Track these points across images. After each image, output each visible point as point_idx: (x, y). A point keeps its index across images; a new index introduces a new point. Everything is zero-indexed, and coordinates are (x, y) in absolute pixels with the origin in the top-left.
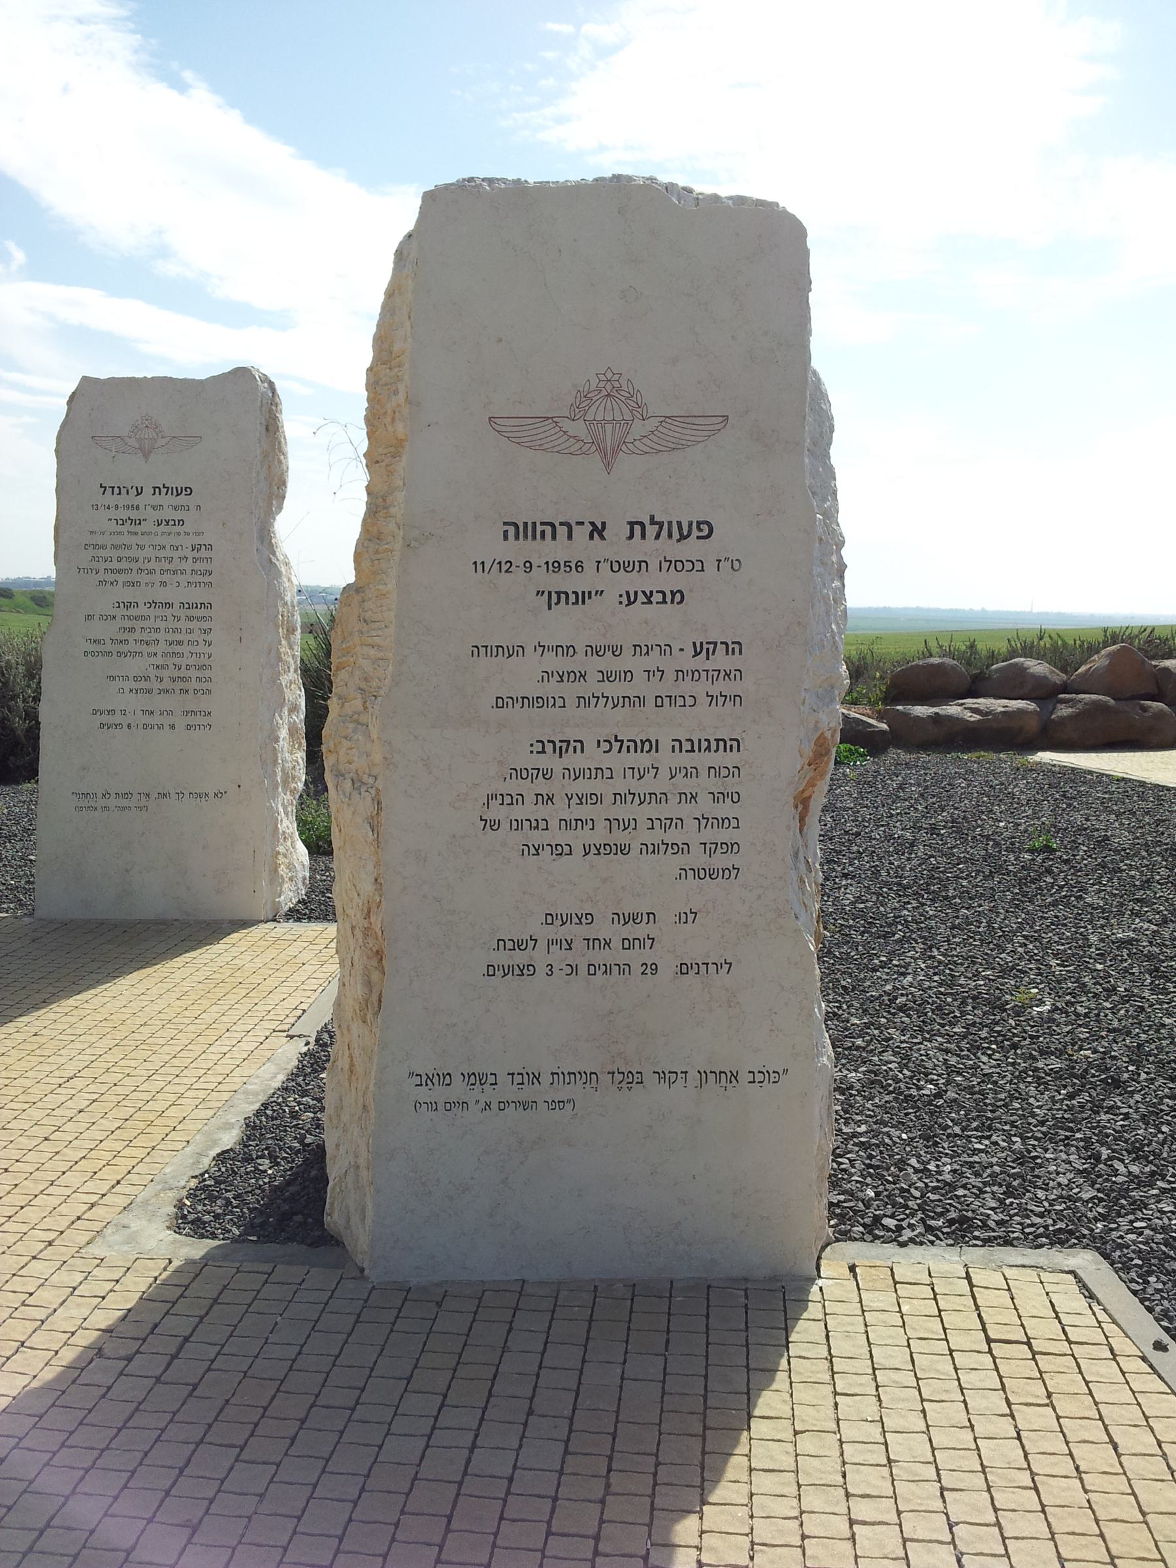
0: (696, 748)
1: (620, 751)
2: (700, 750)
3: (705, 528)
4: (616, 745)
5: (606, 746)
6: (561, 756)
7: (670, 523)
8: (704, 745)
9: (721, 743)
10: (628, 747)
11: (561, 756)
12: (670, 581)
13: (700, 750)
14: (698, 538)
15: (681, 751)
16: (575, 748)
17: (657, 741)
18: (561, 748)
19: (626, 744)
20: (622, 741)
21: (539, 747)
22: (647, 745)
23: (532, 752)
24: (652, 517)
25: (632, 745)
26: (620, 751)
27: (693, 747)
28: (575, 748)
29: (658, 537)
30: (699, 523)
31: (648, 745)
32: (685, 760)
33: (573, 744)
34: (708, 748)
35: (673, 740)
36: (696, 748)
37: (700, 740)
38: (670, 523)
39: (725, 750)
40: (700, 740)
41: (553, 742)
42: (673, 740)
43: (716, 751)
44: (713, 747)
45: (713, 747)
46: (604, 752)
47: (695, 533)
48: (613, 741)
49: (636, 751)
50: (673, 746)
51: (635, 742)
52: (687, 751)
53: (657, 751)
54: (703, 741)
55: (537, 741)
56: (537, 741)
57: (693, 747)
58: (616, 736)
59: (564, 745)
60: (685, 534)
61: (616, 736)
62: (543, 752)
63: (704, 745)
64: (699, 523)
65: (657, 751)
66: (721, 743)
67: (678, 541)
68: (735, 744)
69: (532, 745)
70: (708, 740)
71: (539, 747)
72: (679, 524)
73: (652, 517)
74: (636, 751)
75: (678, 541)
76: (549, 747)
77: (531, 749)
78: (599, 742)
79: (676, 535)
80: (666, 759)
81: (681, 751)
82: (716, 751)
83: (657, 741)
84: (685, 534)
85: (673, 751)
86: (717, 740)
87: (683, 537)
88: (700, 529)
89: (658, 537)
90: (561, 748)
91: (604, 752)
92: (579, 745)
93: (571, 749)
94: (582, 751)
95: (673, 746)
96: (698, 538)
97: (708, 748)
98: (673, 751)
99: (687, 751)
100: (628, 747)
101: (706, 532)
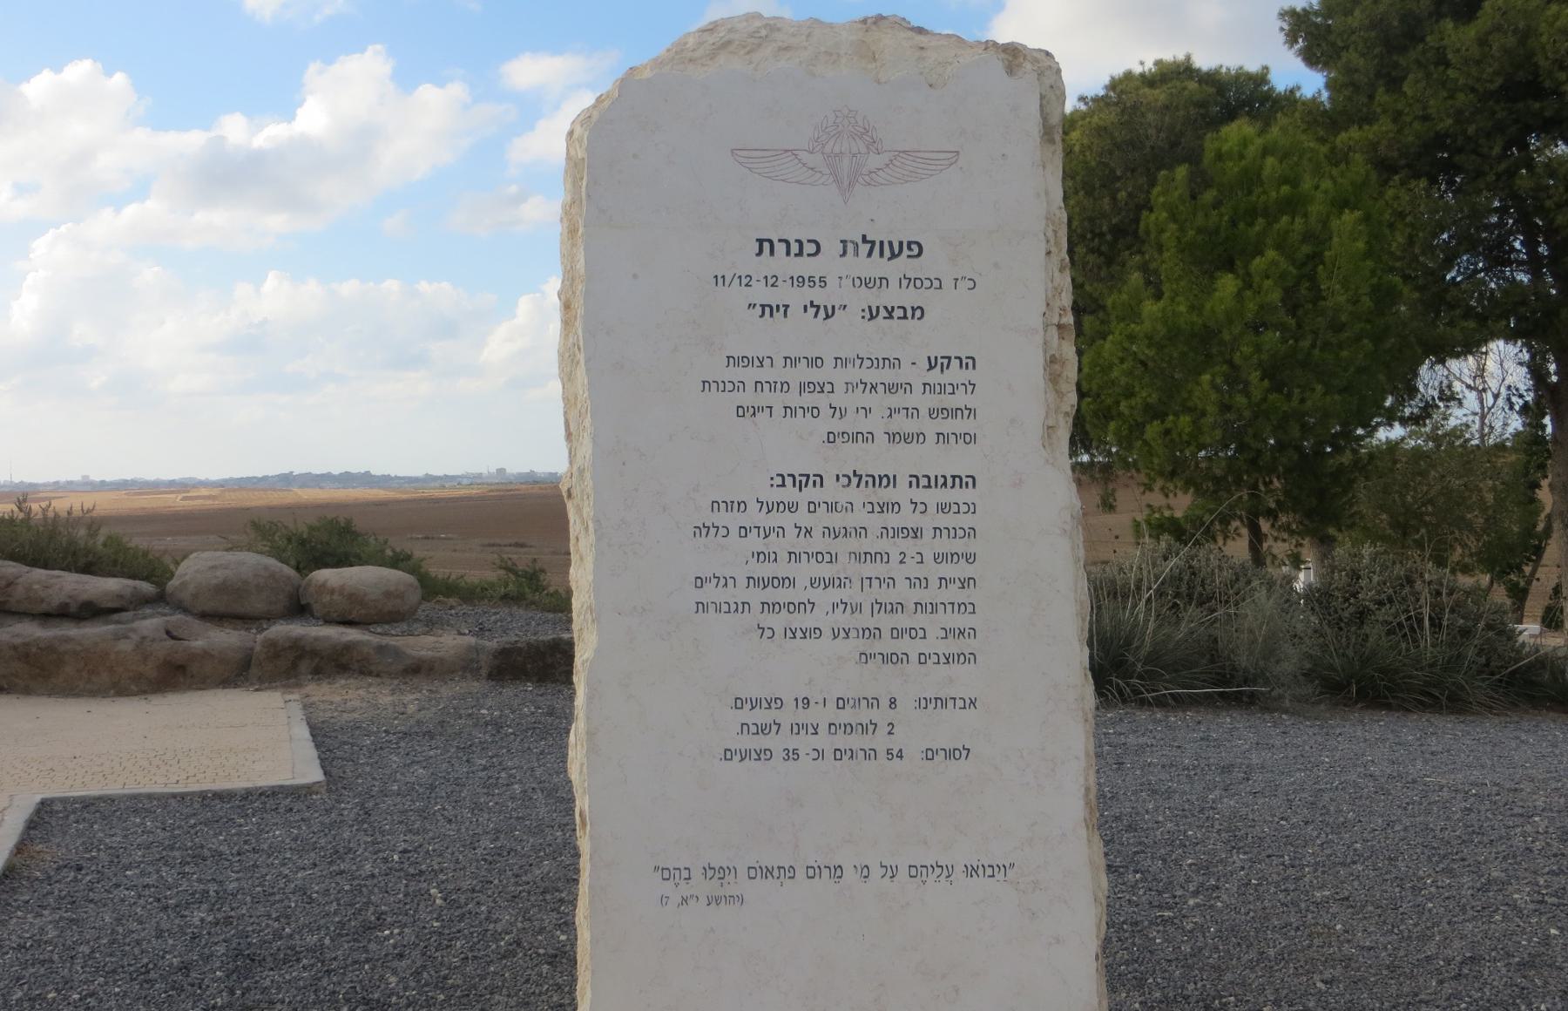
0: (933, 483)
1: (858, 486)
2: (936, 486)
3: (913, 246)
4: (855, 481)
5: (845, 481)
6: (800, 489)
7: (882, 243)
8: (941, 481)
9: (957, 480)
10: (867, 482)
11: (800, 489)
12: (910, 298)
13: (936, 486)
14: (909, 256)
15: (918, 486)
16: (814, 482)
17: (895, 476)
18: (800, 482)
19: (864, 479)
20: (861, 477)
21: (779, 481)
22: (885, 481)
23: (772, 485)
24: (864, 237)
25: (870, 480)
26: (858, 486)
27: (929, 481)
28: (814, 482)
29: (870, 254)
30: (909, 244)
31: (890, 480)
32: (920, 495)
33: (812, 479)
34: (945, 484)
35: (911, 476)
36: (933, 483)
37: (936, 477)
38: (882, 243)
39: (961, 487)
40: (936, 477)
41: (793, 476)
42: (911, 476)
43: (953, 487)
44: (950, 481)
45: (950, 481)
46: (843, 486)
47: (906, 252)
48: (851, 475)
49: (874, 485)
50: (911, 482)
51: (874, 477)
52: (924, 487)
53: (894, 486)
54: (939, 478)
55: (778, 475)
56: (778, 475)
57: (929, 481)
58: (855, 471)
59: (804, 479)
60: (896, 253)
61: (855, 471)
62: (783, 485)
63: (941, 481)
64: (909, 244)
65: (894, 486)
66: (957, 480)
67: (889, 259)
68: (970, 480)
69: (772, 479)
70: (944, 477)
71: (779, 481)
72: (891, 244)
73: (864, 237)
74: (874, 485)
75: (889, 259)
76: (789, 481)
77: (772, 482)
78: (838, 476)
79: (887, 253)
80: (902, 493)
81: (918, 486)
82: (953, 487)
83: (895, 476)
84: (896, 251)
85: (911, 486)
86: (954, 477)
87: (893, 256)
88: (910, 248)
89: (870, 254)
90: (800, 482)
91: (843, 486)
92: (818, 479)
93: (811, 482)
94: (822, 485)
95: (911, 482)
96: (909, 256)
97: (945, 484)
98: (911, 486)
99: (924, 487)
100: (867, 482)
101: (916, 251)
